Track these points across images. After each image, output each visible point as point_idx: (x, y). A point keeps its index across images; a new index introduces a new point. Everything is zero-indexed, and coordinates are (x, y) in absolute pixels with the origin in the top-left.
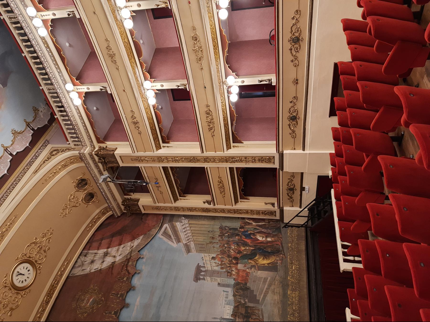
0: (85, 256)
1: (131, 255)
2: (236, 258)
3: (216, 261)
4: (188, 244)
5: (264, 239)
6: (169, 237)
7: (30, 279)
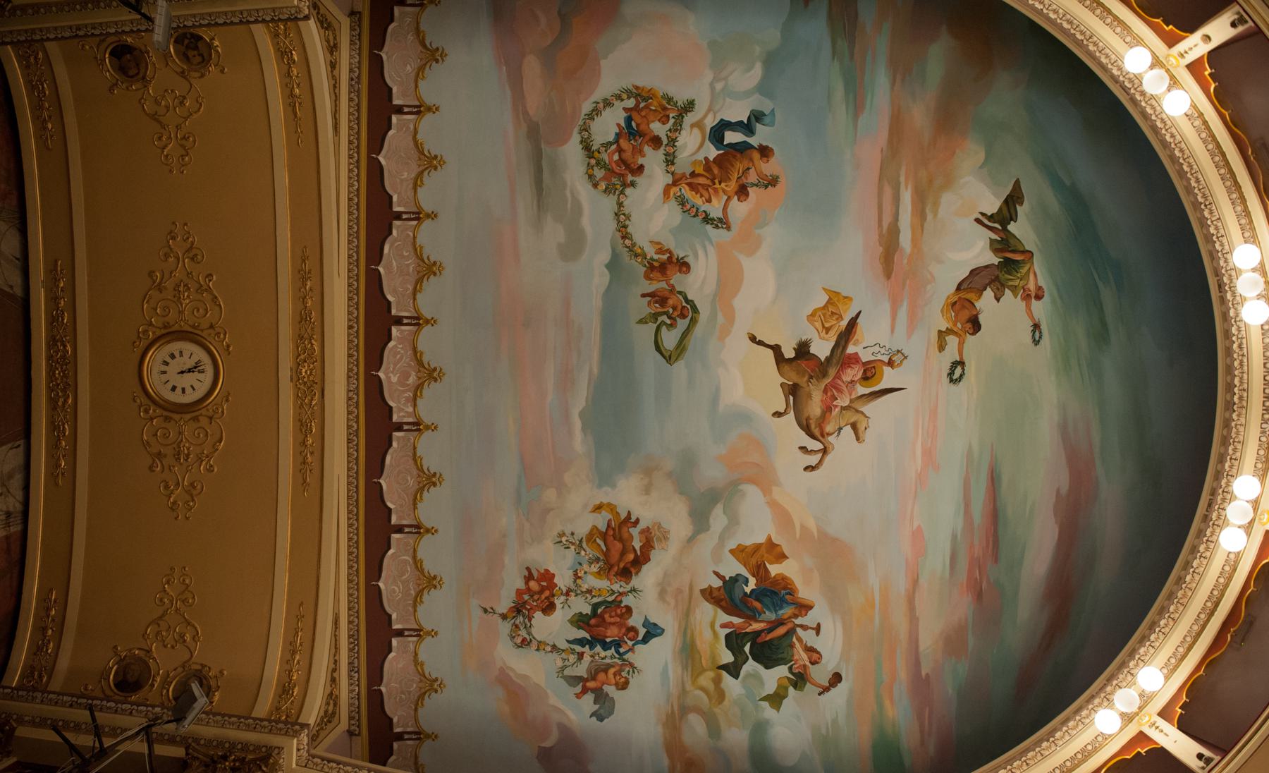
0: (8, 514)
7: (155, 371)
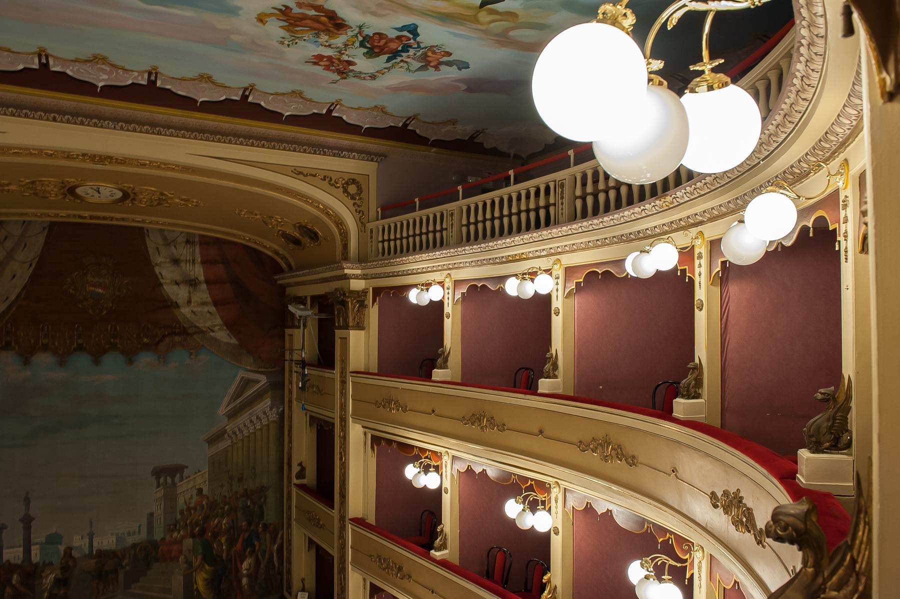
1: (195, 333)
2: (203, 532)
3: (195, 498)
4: (226, 436)
5: (245, 572)
6: (238, 394)
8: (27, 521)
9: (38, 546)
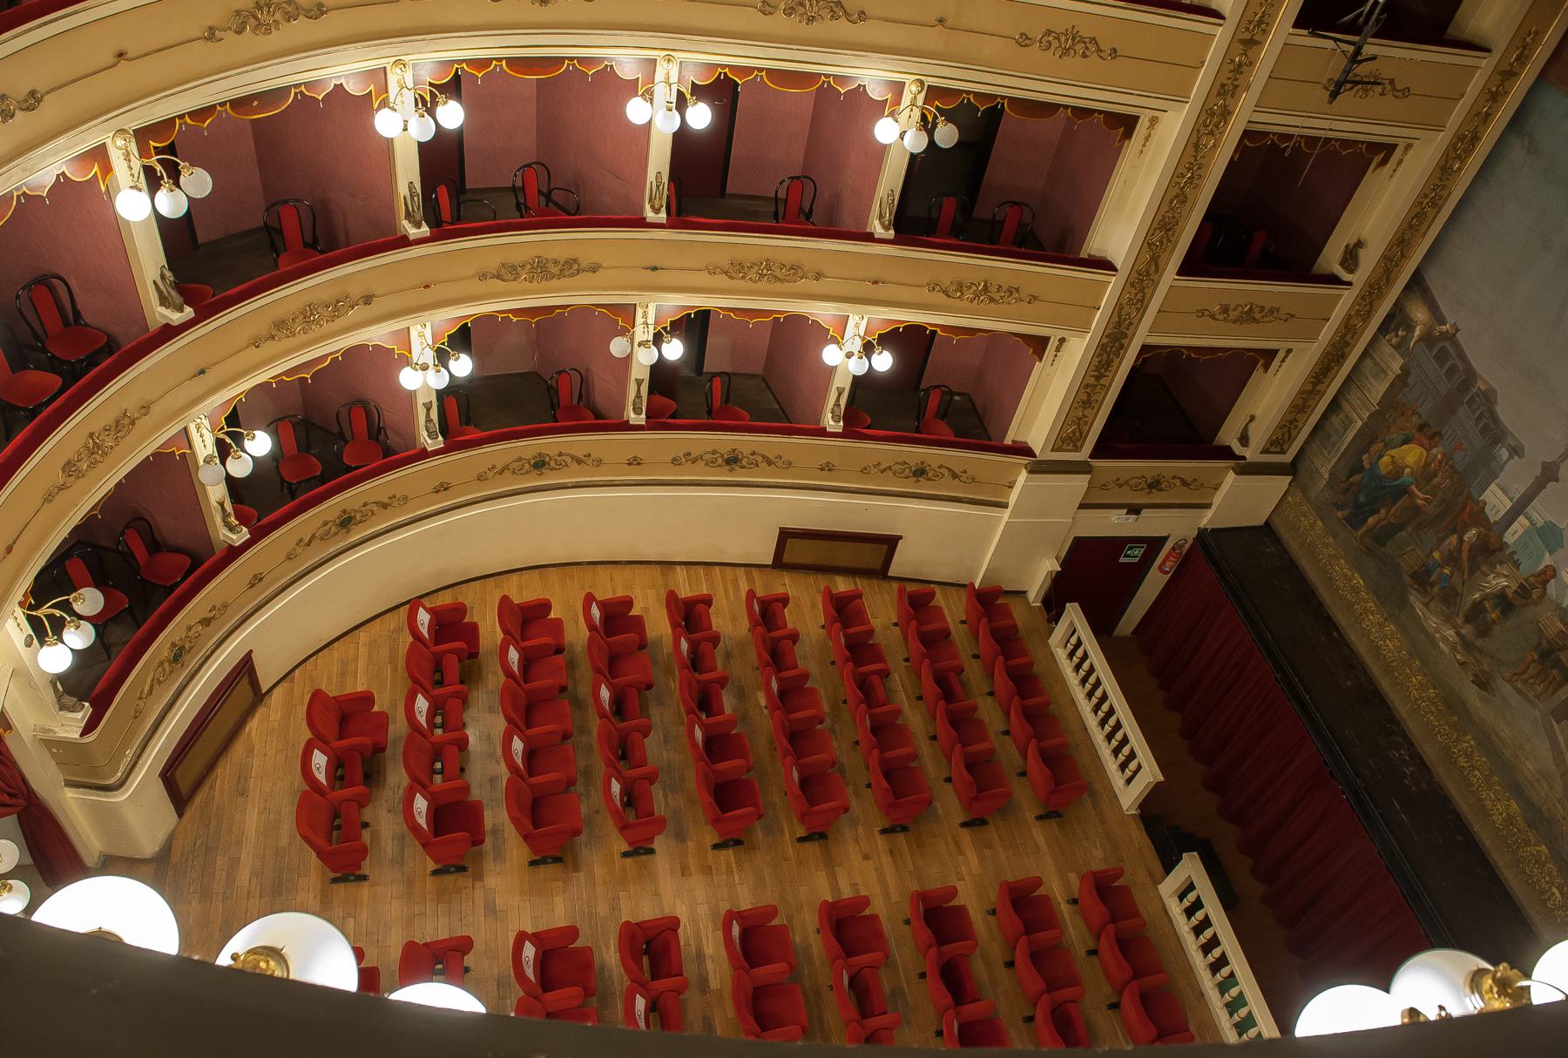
8: (1549, 474)
9: (1528, 523)
